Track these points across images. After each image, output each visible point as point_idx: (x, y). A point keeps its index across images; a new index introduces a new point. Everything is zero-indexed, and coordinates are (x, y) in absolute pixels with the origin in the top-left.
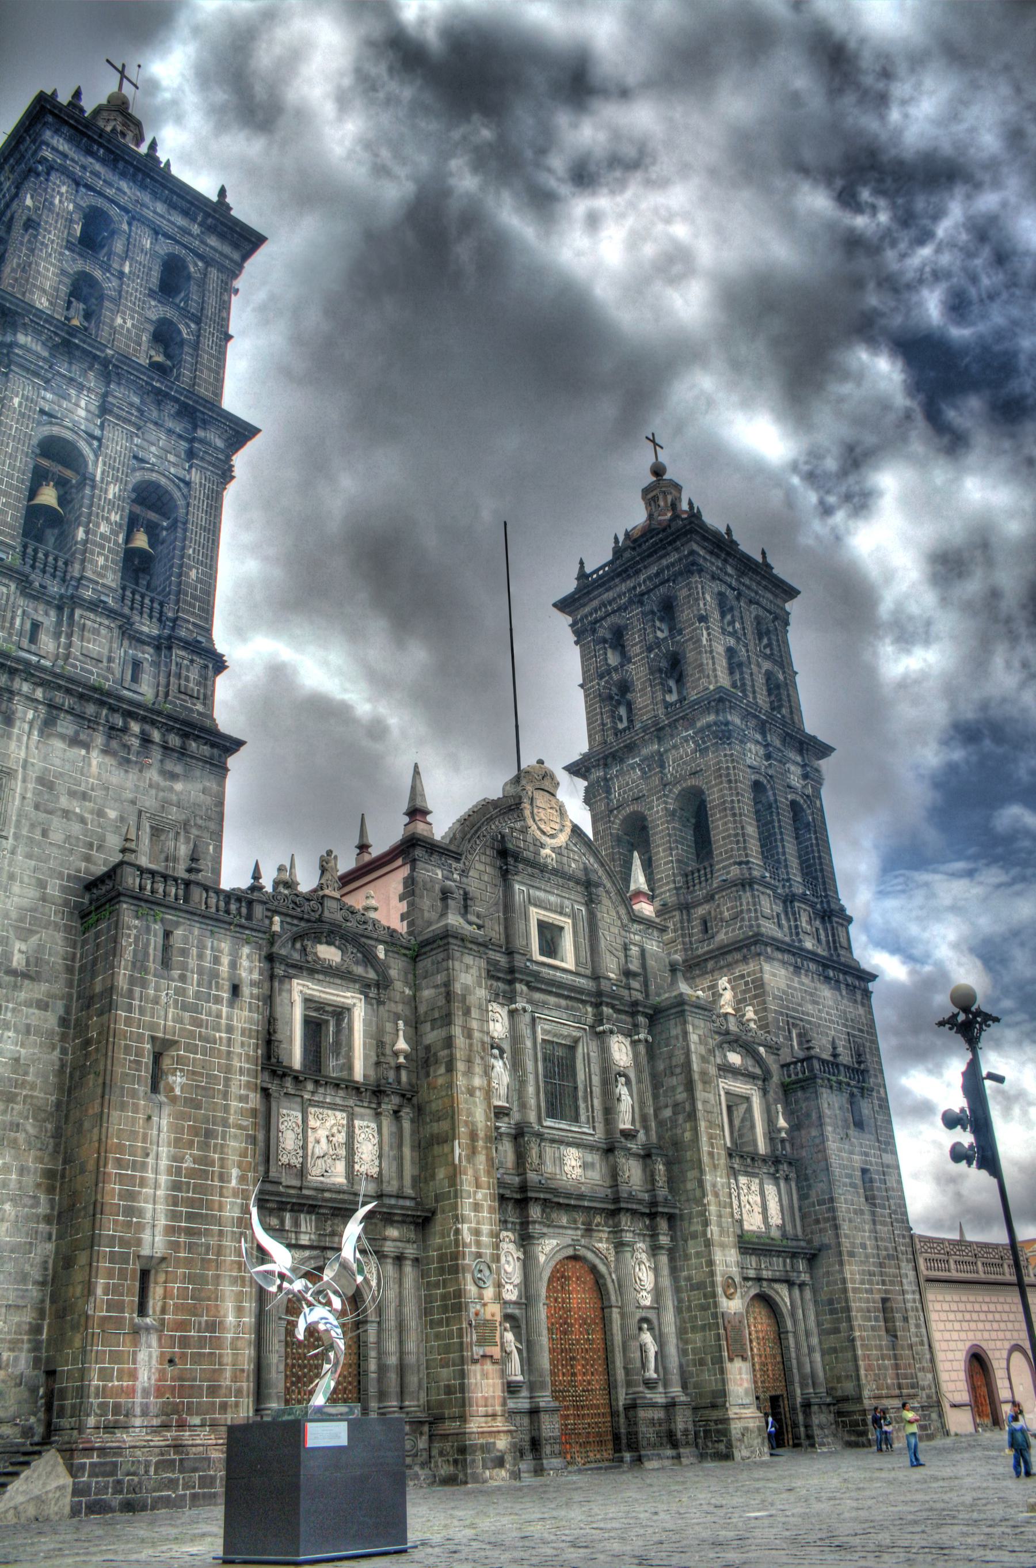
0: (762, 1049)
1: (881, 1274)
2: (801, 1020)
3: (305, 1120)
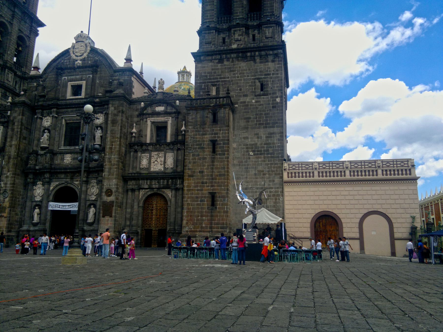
0: (177, 101)
1: (212, 182)
2: (218, 82)
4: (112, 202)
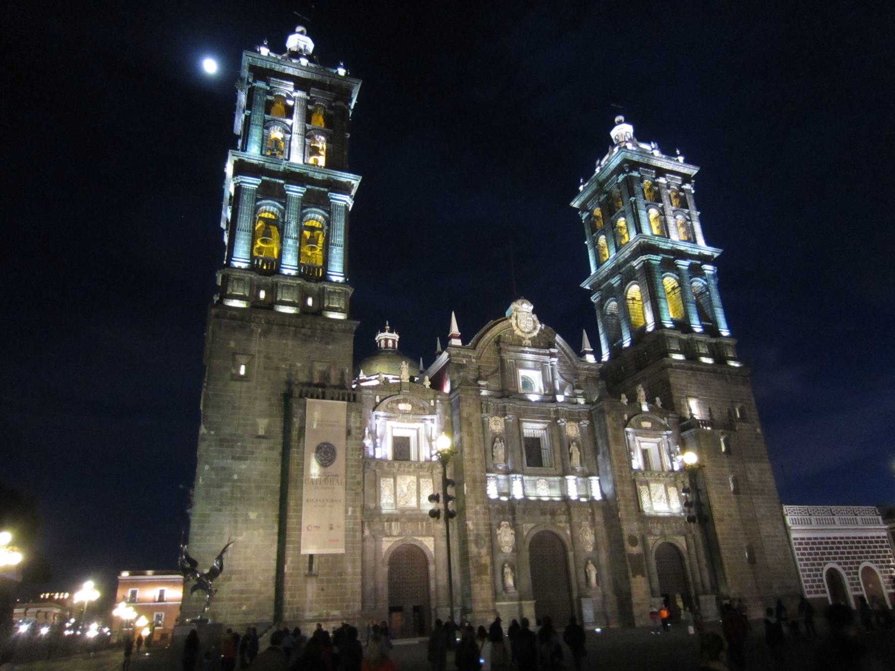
3: (395, 482)
4: (639, 555)
